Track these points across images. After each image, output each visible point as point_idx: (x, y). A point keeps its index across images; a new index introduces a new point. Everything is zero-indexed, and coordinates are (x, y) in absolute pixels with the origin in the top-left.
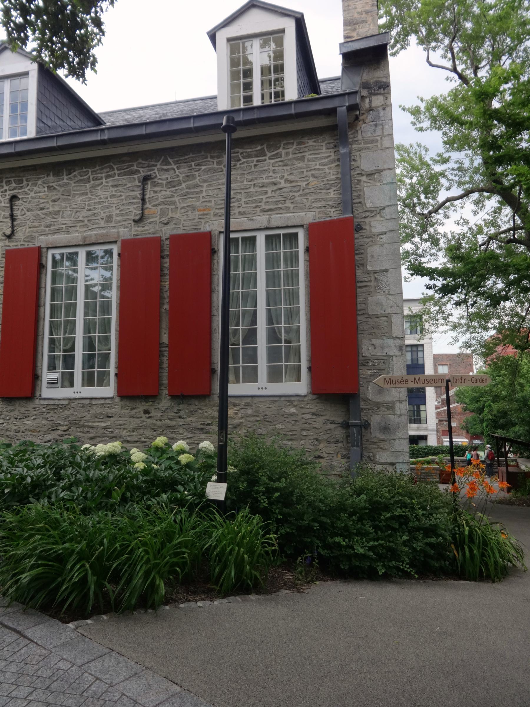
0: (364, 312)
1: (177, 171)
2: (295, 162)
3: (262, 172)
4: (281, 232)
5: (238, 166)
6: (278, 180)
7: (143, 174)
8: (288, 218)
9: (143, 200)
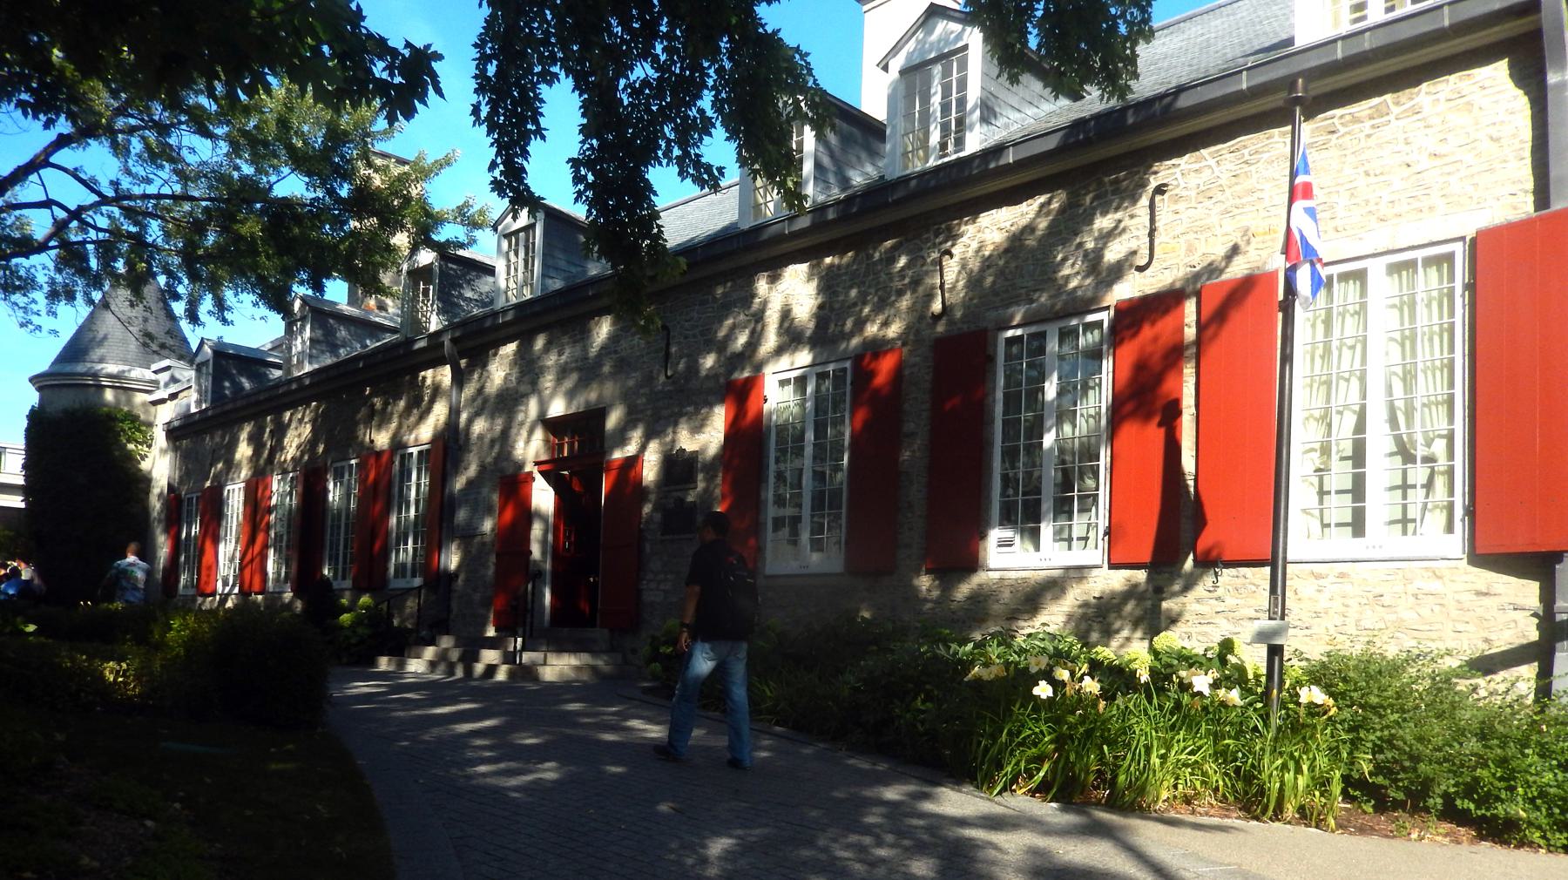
1: (1216, 169)
4: (1419, 255)
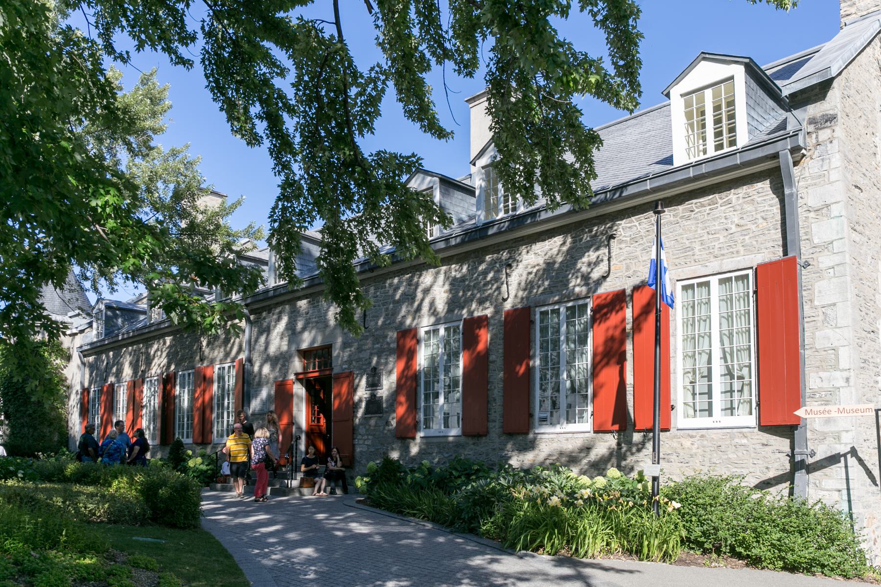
0: (811, 346)
1: (639, 227)
2: (745, 206)
3: (714, 219)
4: (733, 275)
5: (693, 216)
6: (729, 225)
8: (739, 261)
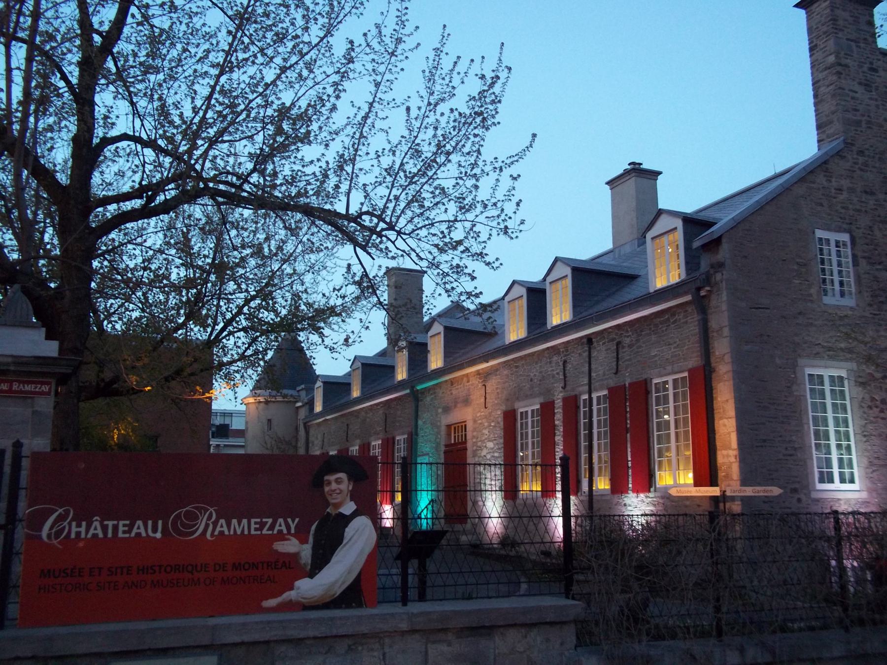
7: (618, 340)
9: (618, 358)
